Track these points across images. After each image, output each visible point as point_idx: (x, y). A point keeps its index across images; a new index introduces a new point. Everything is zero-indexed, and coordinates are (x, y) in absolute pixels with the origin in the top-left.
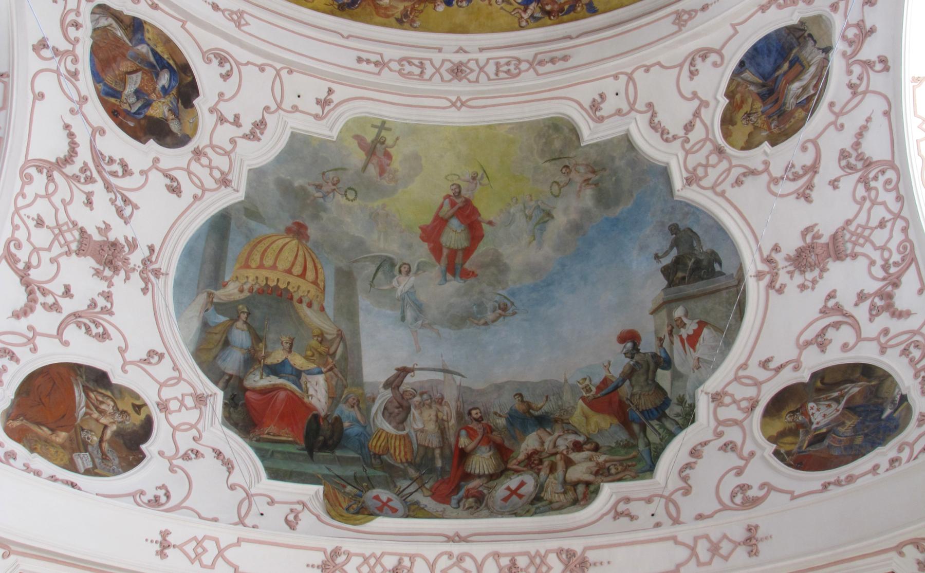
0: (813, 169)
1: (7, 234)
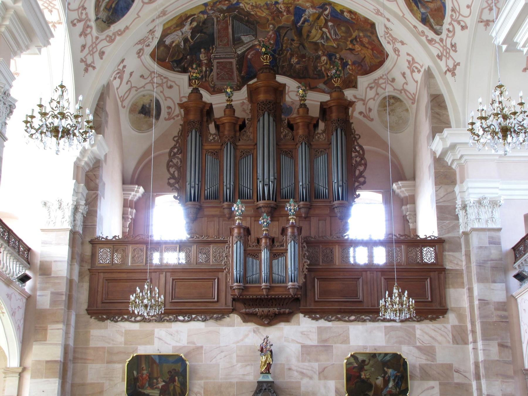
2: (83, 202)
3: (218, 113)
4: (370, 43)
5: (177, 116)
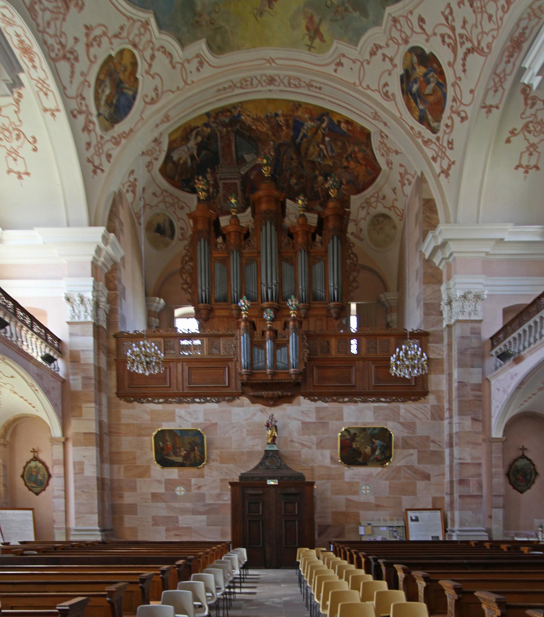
2: (103, 299)
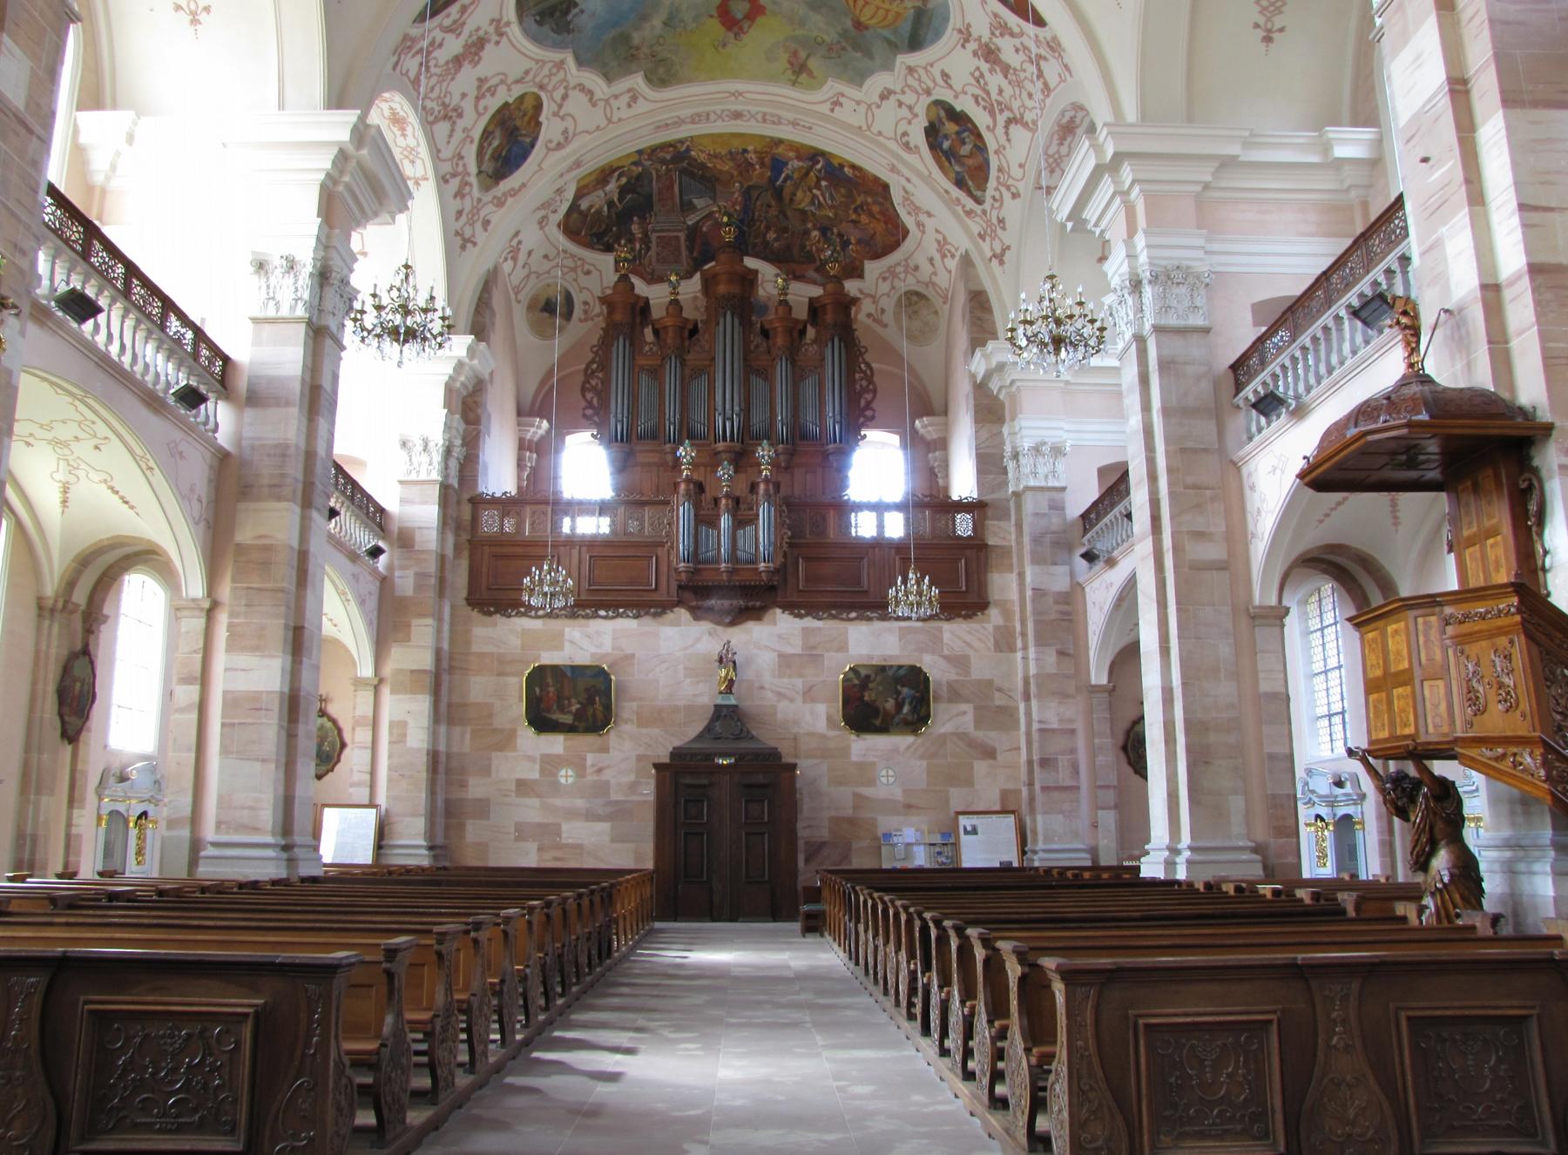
0: (478, 99)
1: (1048, 101)
2: (458, 442)
3: (657, 312)
4: (882, 213)
5: (598, 315)
